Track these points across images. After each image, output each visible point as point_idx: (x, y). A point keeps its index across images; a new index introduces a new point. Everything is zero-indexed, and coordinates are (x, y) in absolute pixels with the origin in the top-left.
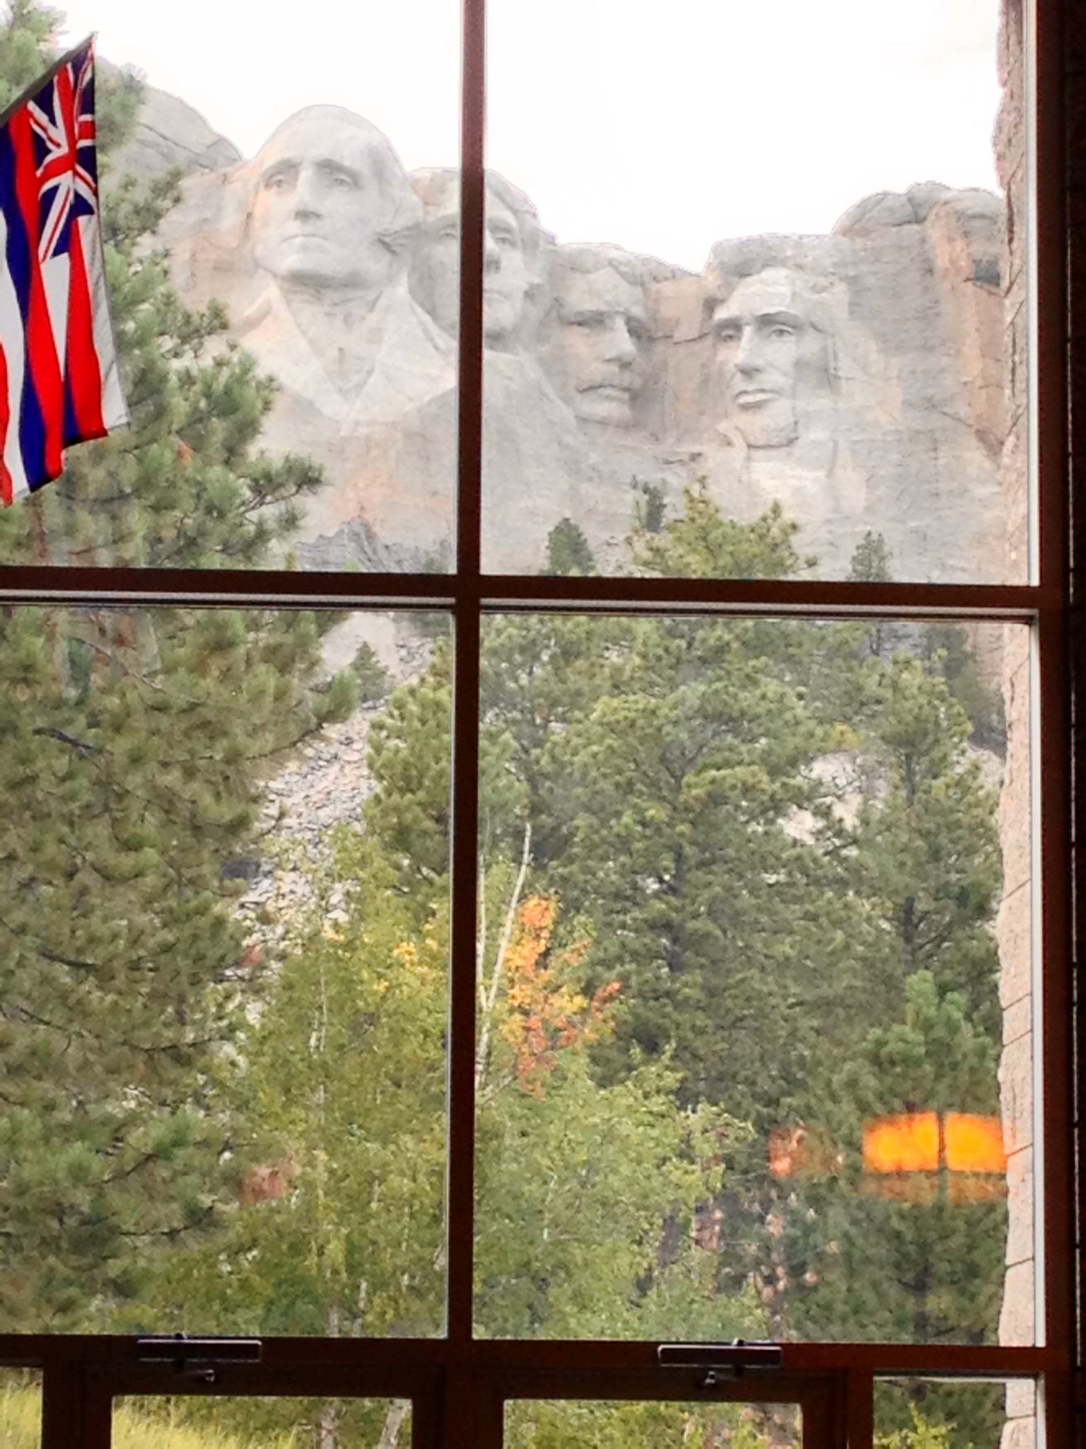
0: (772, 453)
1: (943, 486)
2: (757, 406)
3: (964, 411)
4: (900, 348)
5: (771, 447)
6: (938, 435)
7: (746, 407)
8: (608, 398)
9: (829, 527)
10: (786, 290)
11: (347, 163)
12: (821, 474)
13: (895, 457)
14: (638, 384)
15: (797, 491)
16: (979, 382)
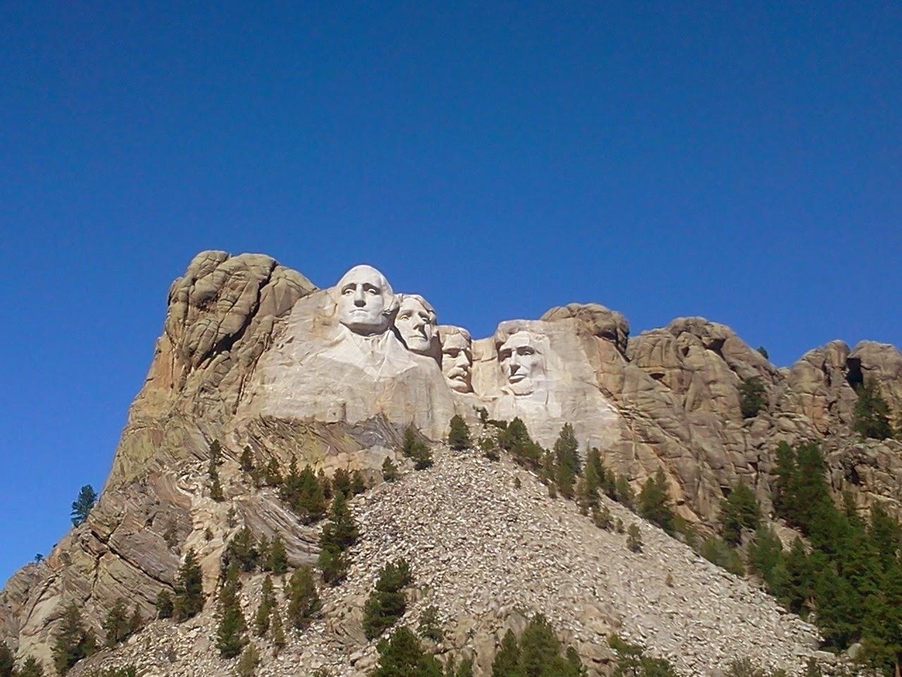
0: (523, 396)
1: (588, 408)
2: (519, 380)
3: (595, 381)
4: (569, 360)
5: (524, 395)
6: (586, 390)
7: (513, 382)
8: (459, 380)
9: (549, 422)
10: (528, 338)
11: (374, 285)
12: (544, 403)
13: (571, 398)
15: (537, 409)
16: (601, 371)
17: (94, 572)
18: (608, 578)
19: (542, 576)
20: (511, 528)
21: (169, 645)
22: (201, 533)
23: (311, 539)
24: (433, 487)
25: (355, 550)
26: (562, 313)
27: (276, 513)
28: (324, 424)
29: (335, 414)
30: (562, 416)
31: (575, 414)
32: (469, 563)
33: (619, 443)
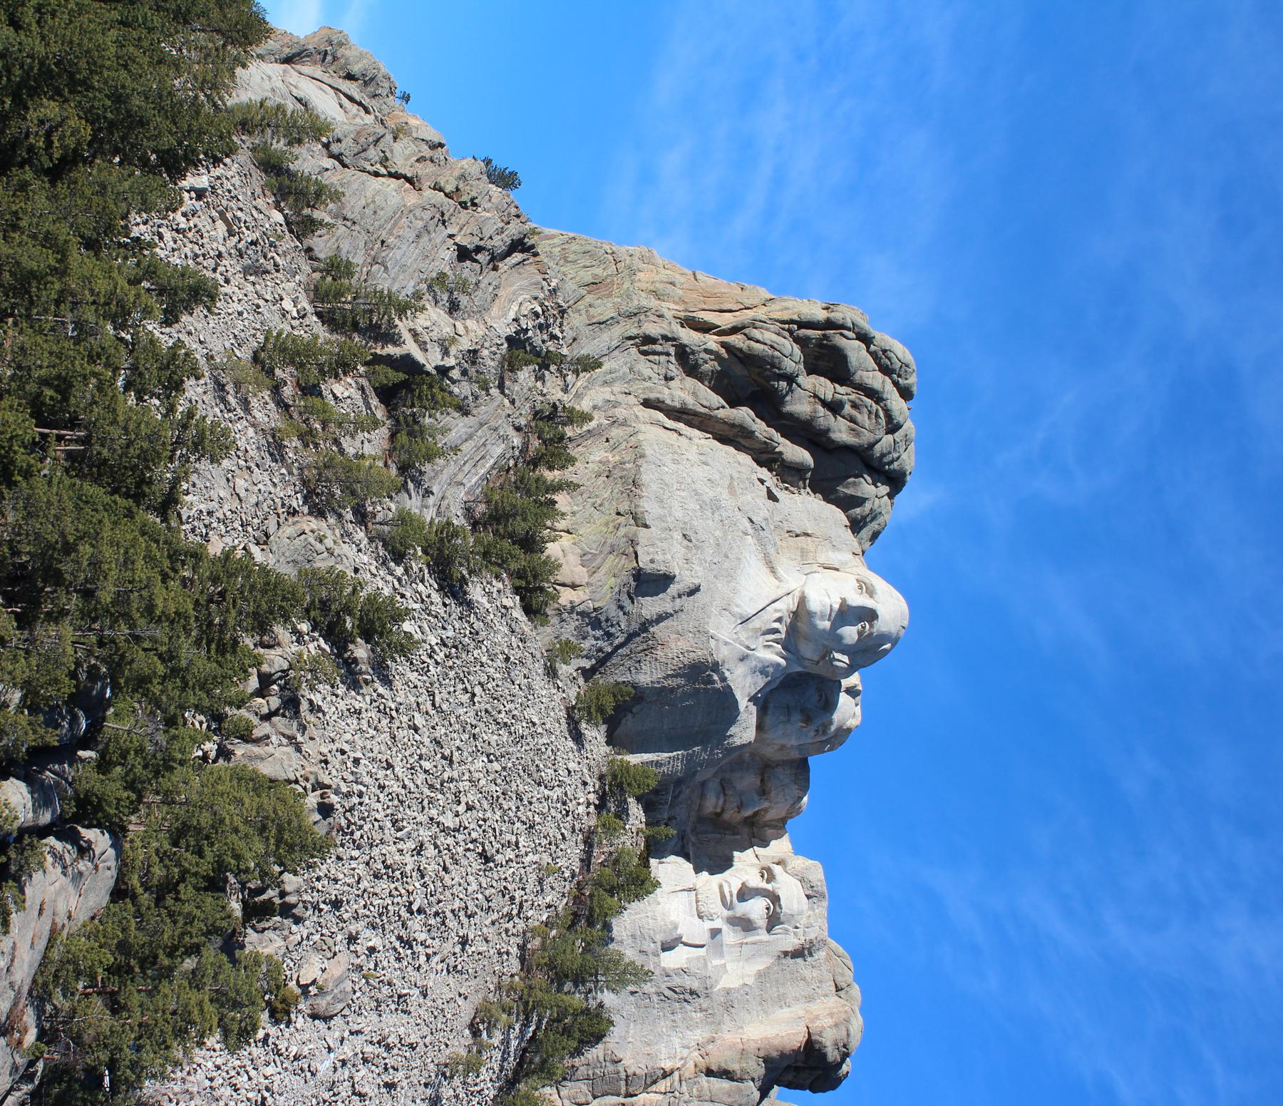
8: (718, 798)
13: (695, 985)
14: (726, 816)
17: (383, 171)
18: (393, 1007)
19: (393, 886)
20: (471, 846)
21: (270, 267)
22: (448, 330)
23: (443, 509)
24: (535, 720)
25: (427, 576)
26: (843, 975)
27: (483, 458)
28: (633, 542)
29: (652, 561)
30: (664, 969)
31: (668, 993)
32: (411, 761)
33: (621, 1069)
